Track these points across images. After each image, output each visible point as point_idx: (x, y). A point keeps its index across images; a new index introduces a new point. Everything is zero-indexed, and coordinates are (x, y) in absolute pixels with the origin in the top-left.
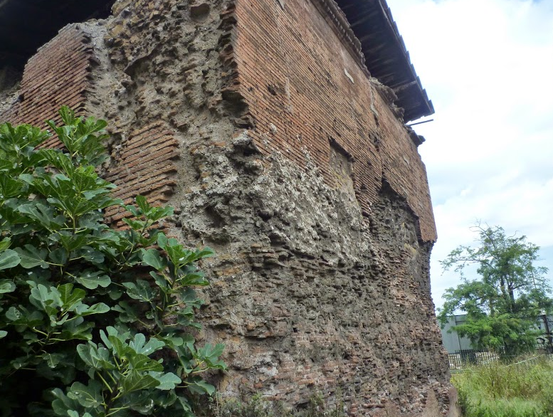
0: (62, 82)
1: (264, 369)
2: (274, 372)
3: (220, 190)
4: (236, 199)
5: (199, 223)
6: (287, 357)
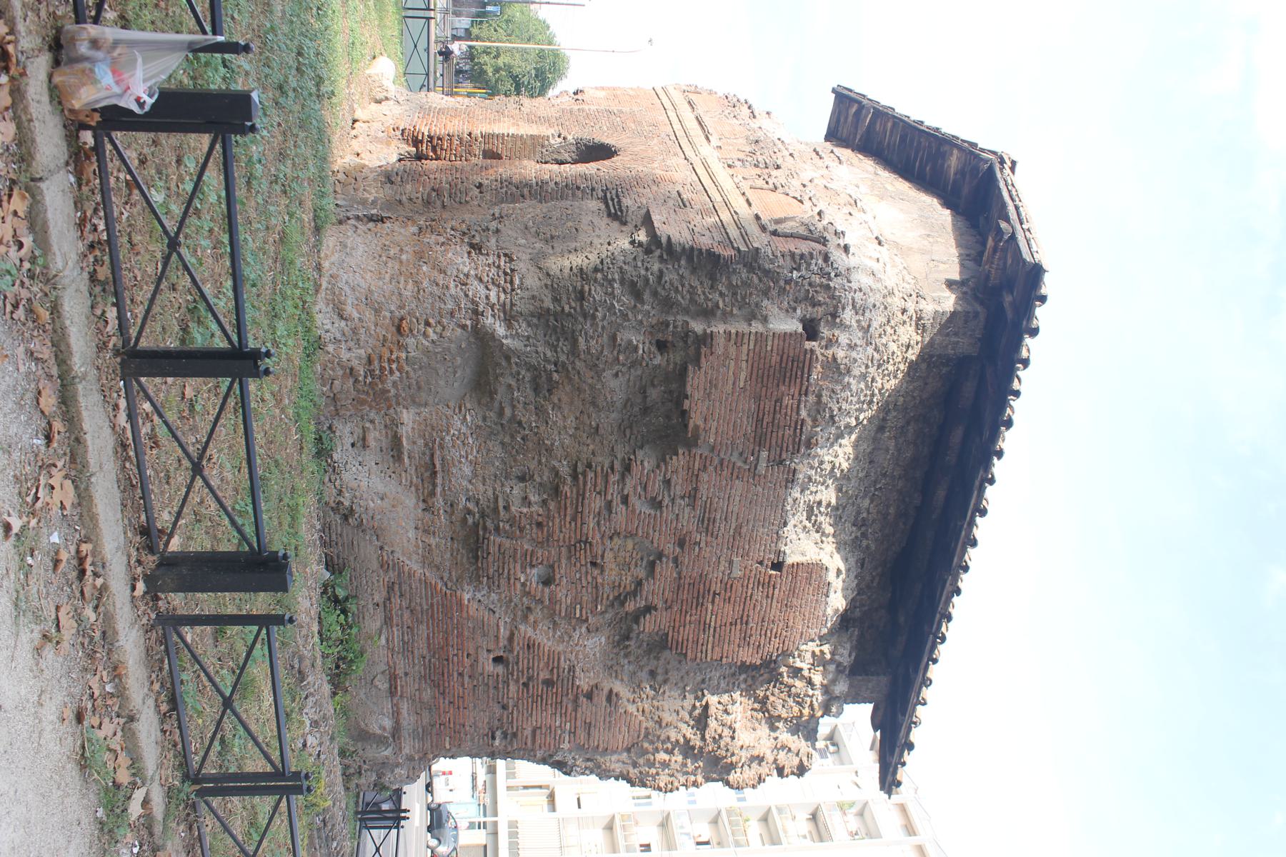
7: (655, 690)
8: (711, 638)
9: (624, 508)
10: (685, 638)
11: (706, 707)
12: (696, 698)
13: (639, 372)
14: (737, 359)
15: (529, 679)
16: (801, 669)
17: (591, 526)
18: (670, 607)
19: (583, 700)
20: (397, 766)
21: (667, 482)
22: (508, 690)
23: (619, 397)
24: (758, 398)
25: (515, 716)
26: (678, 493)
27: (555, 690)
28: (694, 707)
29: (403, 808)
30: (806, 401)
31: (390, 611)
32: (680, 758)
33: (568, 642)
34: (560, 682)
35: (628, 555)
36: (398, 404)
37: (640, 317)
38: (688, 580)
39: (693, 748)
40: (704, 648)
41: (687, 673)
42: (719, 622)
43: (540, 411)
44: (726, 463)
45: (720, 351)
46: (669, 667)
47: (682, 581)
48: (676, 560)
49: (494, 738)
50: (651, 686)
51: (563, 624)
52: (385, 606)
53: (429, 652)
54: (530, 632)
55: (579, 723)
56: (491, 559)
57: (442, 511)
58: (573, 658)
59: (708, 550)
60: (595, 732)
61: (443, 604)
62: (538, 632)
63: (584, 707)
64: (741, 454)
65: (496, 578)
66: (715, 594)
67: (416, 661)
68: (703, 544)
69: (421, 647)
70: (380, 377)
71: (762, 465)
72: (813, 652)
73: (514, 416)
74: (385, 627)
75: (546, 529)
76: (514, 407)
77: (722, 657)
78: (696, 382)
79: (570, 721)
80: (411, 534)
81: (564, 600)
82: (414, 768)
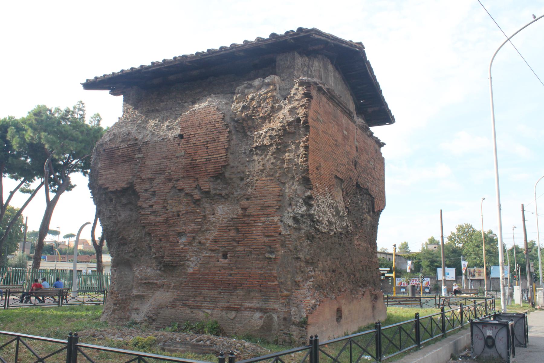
0: (211, 137)
1: (310, 272)
2: (313, 273)
3: (300, 212)
5: (290, 222)
6: (316, 269)
7: (249, 176)
8: (214, 156)
9: (154, 206)
10: (213, 168)
11: (256, 148)
12: (253, 154)
13: (119, 207)
14: (106, 175)
15: (234, 240)
16: (244, 107)
17: (160, 218)
18: (197, 179)
19: (249, 212)
20: (290, 313)
21: (146, 190)
22: (239, 251)
23: (128, 213)
24: (119, 164)
25: (255, 247)
26: (149, 186)
27: (240, 228)
28: (257, 154)
30: (123, 146)
31: (194, 306)
32: (287, 154)
33: (216, 223)
34: (235, 225)
35: (174, 201)
36: (130, 295)
37: (104, 210)
38: (185, 174)
39: (277, 149)
40: (219, 158)
41: (240, 162)
42: (206, 155)
43: (131, 243)
44: (139, 170)
45: (104, 181)
46: (236, 172)
47: (185, 176)
48: (177, 180)
49: (270, 258)
50: (248, 179)
51: (205, 227)
52: (193, 308)
53: (216, 289)
54: (209, 242)
55: (261, 213)
56: (172, 260)
57: (163, 281)
58: (226, 220)
59: (172, 168)
60: (268, 203)
61: (192, 282)
62: (210, 238)
63: (250, 211)
64: (136, 165)
65: (180, 258)
66: (192, 160)
67: (221, 296)
68: (170, 171)
69: (214, 293)
70: (118, 301)
71: (140, 156)
72: (237, 103)
73: (132, 252)
74: (201, 309)
75: (161, 237)
76: (130, 252)
77: (225, 148)
78: (112, 188)
79: (260, 218)
80: (168, 294)
81: (193, 227)
82: (294, 304)
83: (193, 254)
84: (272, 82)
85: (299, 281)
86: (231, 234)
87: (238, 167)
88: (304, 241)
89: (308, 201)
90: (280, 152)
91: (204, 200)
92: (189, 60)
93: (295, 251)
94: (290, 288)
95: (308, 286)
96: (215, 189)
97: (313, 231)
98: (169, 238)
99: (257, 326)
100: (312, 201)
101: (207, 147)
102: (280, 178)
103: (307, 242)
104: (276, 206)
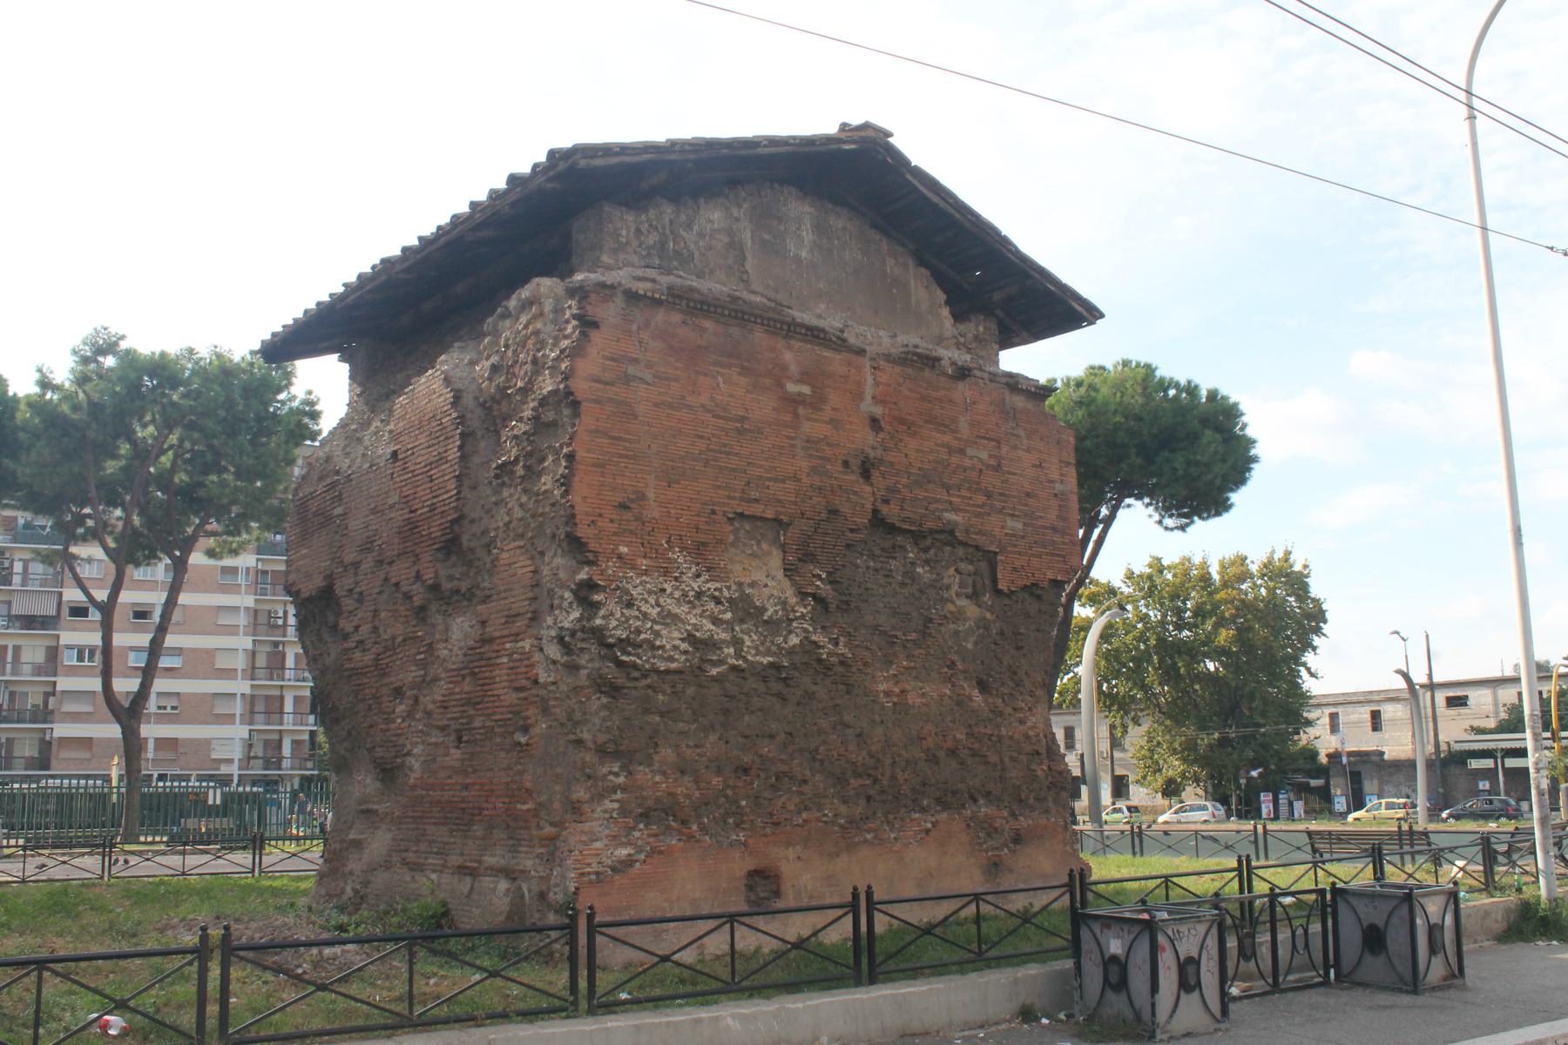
1: (611, 777)
2: (621, 779)
3: (566, 625)
4: (579, 634)
5: (553, 651)
16: (495, 369)
25: (498, 717)
29: (850, 899)
55: (505, 632)
66: (411, 512)
79: (504, 643)
83: (418, 740)
84: (534, 296)
85: (578, 801)
86: (467, 689)
87: (481, 519)
88: (589, 699)
89: (585, 593)
90: (534, 477)
91: (433, 607)
92: (398, 268)
93: (569, 724)
94: (557, 819)
95: (605, 811)
96: (451, 578)
97: (609, 670)
98: (381, 703)
99: (501, 913)
100: (597, 593)
101: (431, 476)
102: (536, 541)
103: (599, 699)
104: (527, 612)
